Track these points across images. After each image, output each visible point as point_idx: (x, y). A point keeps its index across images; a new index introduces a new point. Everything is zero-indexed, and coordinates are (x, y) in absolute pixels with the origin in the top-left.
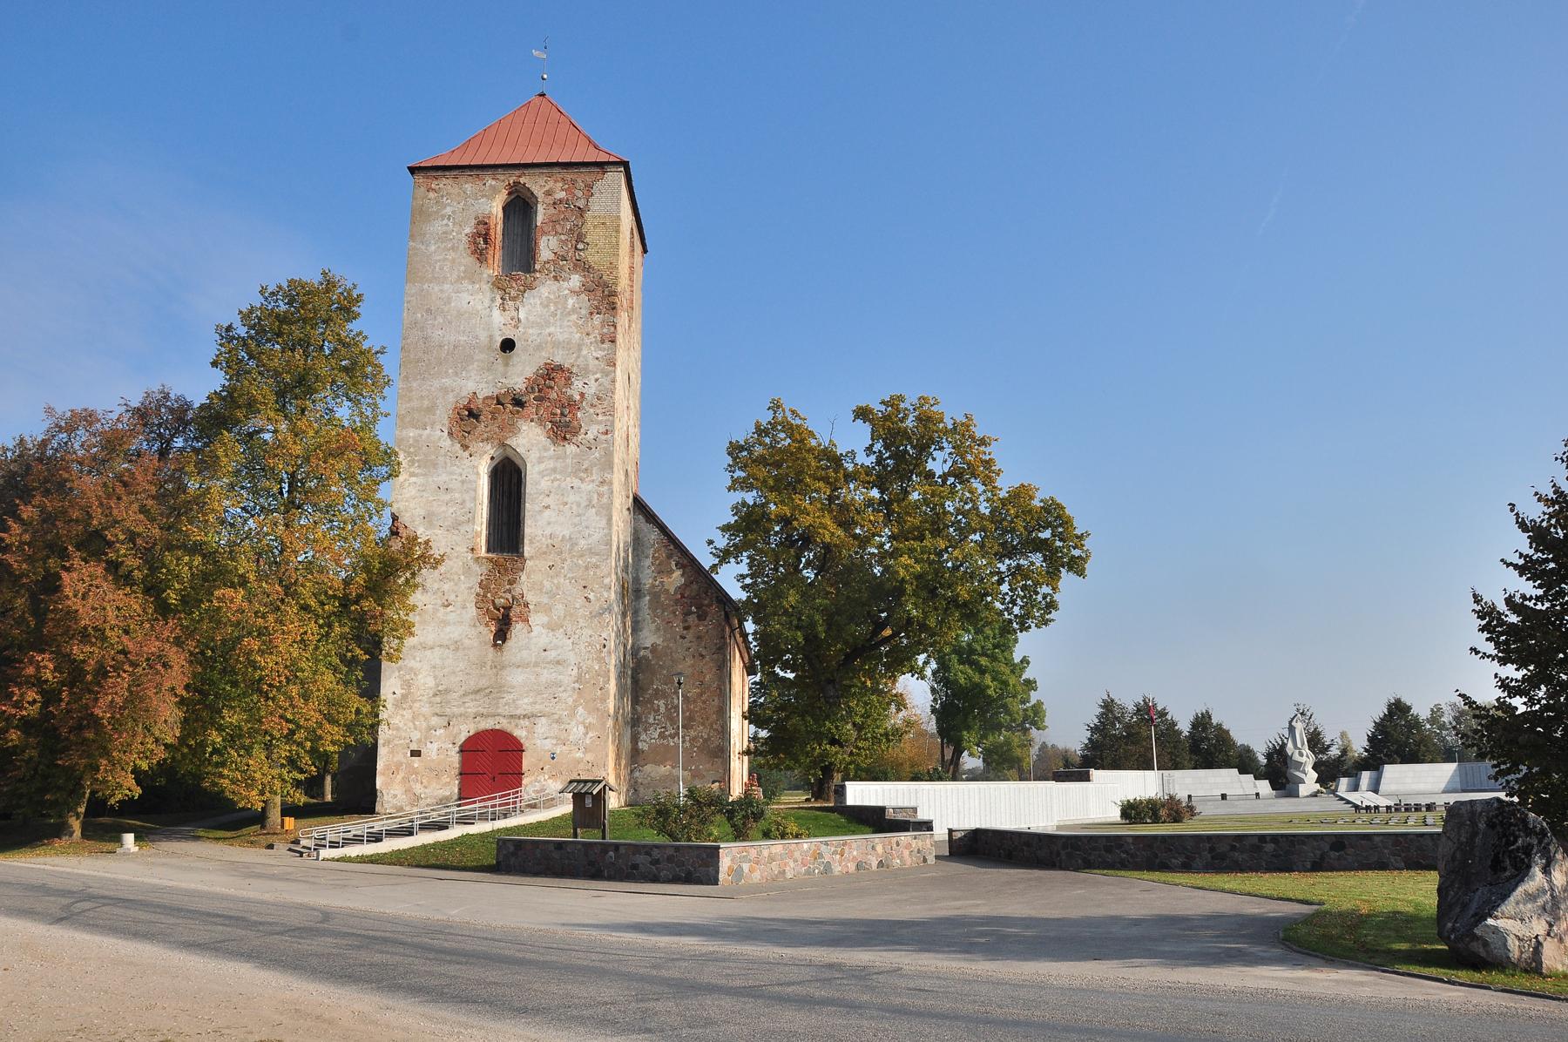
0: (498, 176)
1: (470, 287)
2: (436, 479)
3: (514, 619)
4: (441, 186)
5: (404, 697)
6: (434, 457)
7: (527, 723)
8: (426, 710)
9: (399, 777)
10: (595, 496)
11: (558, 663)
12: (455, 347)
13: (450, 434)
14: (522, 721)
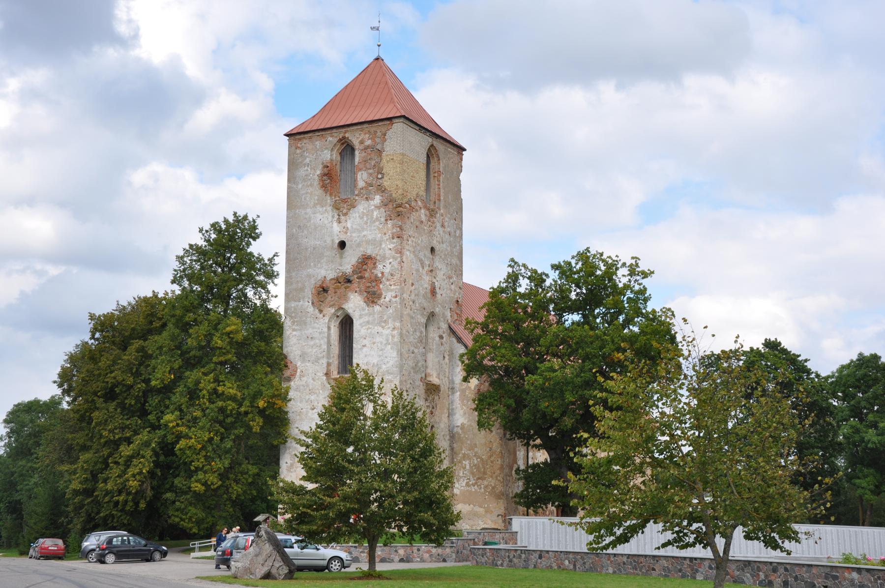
1: (321, 210)
4: (303, 144)
10: (391, 337)
12: (314, 249)
13: (313, 303)
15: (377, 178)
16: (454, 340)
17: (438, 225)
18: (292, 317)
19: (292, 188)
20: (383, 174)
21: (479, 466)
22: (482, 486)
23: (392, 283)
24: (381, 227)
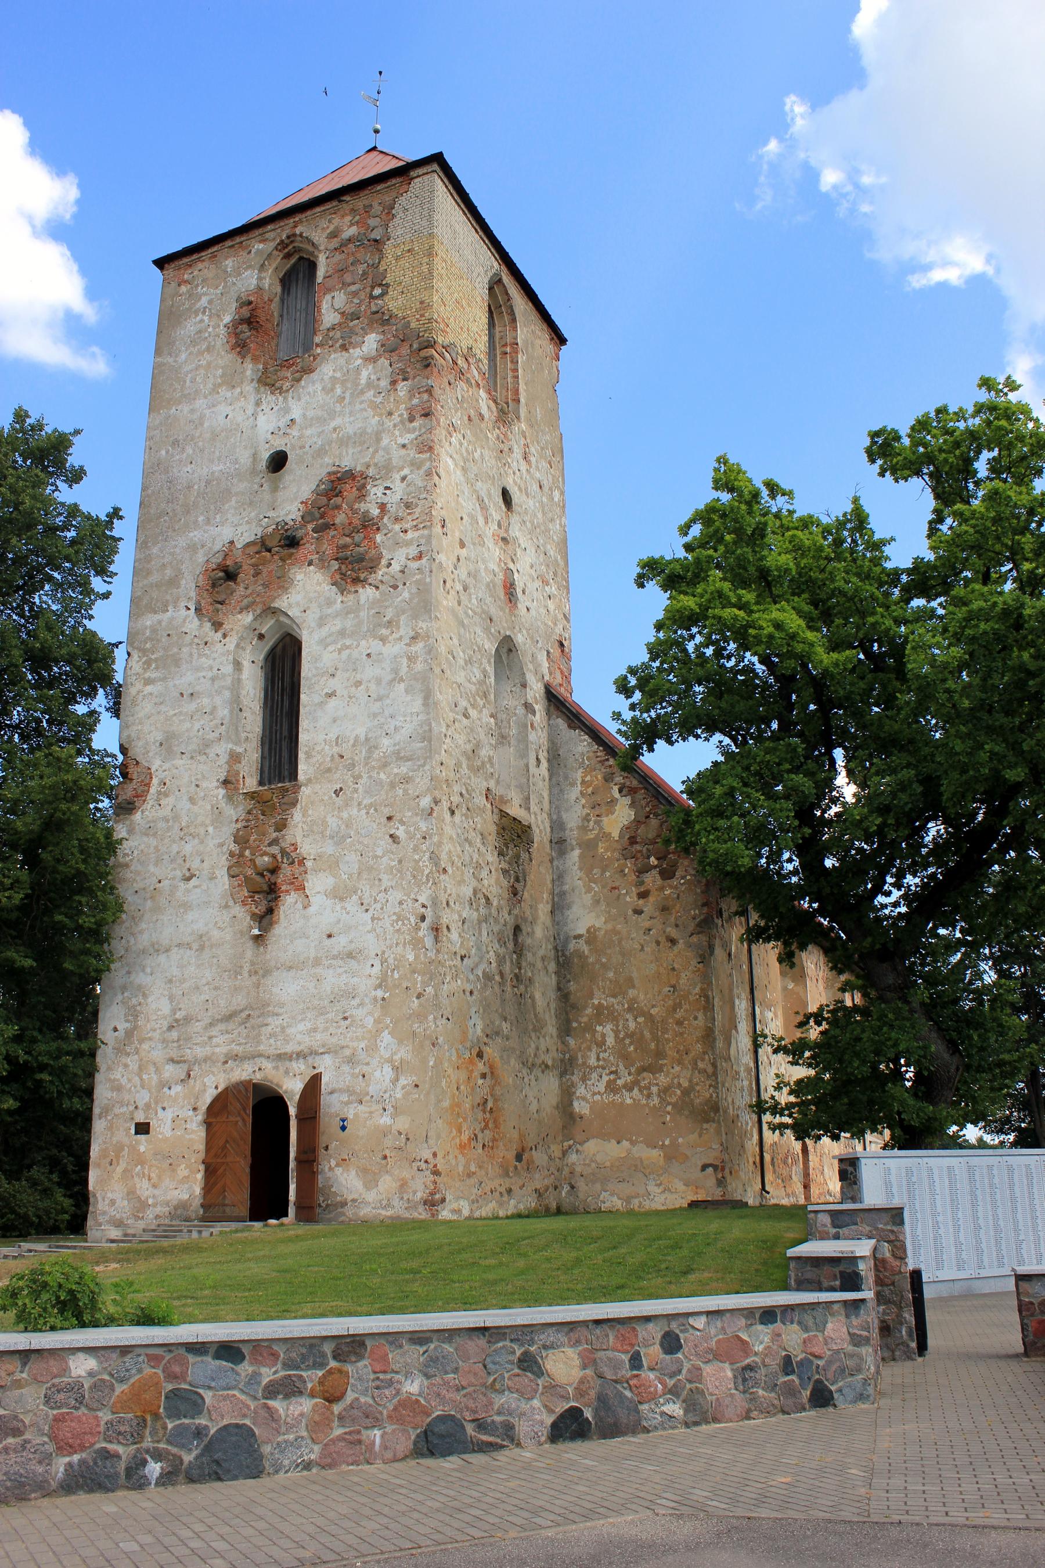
0: (267, 235)
1: (229, 394)
2: (177, 682)
3: (283, 888)
4: (196, 273)
5: (129, 1034)
6: (175, 650)
7: (303, 1067)
8: (158, 1054)
9: (119, 1169)
10: (405, 661)
11: (350, 955)
13: (198, 610)
14: (294, 1064)
15: (372, 297)
16: (561, 723)
18: (143, 651)
19: (164, 364)
20: (387, 285)
21: (642, 1035)
22: (654, 1089)
23: (408, 526)
24: (379, 400)
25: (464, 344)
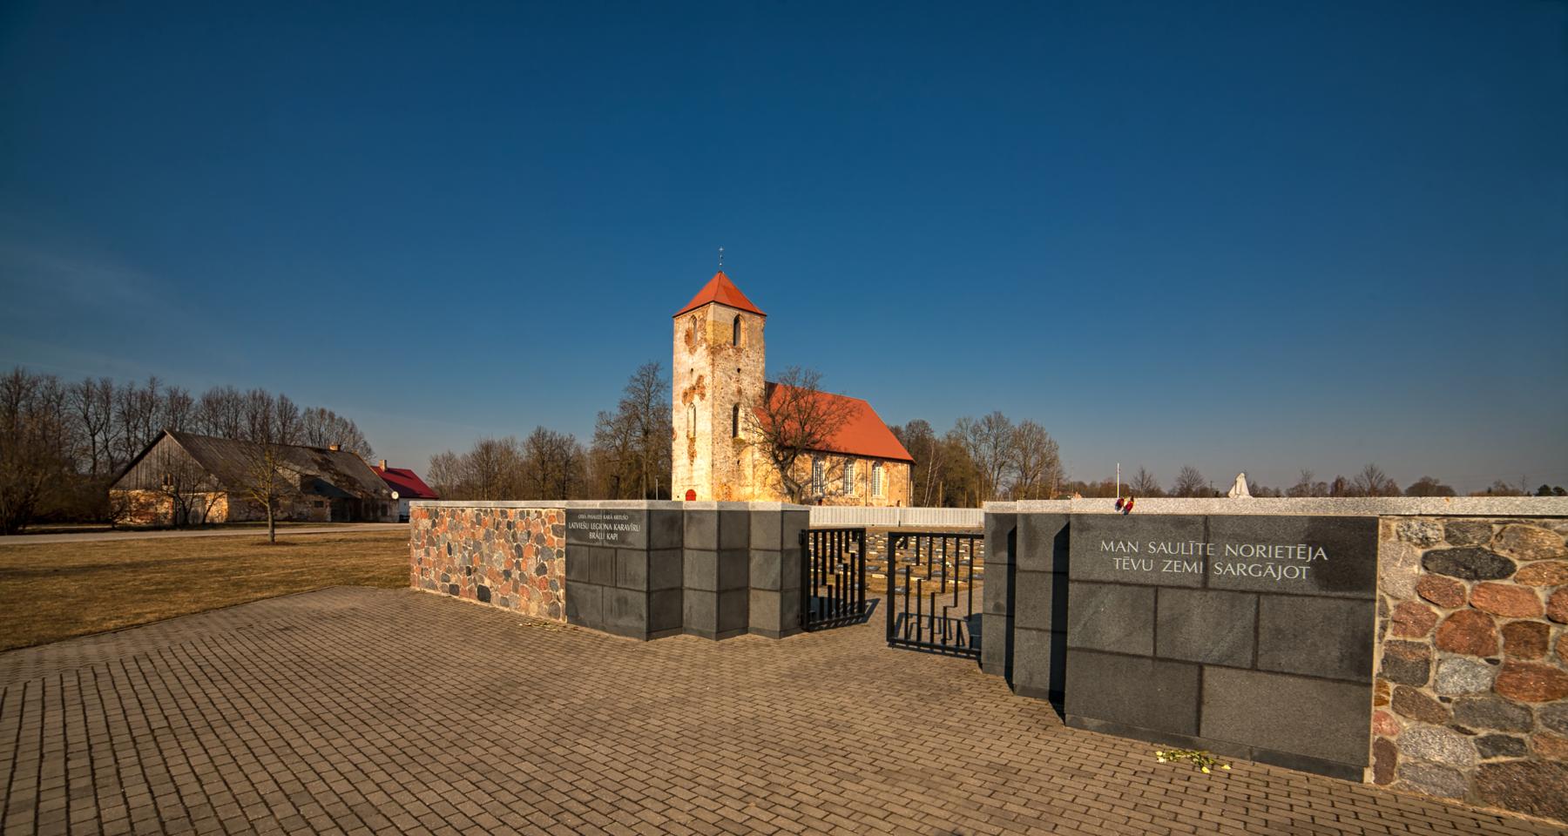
17: (744, 357)
25: (724, 340)
